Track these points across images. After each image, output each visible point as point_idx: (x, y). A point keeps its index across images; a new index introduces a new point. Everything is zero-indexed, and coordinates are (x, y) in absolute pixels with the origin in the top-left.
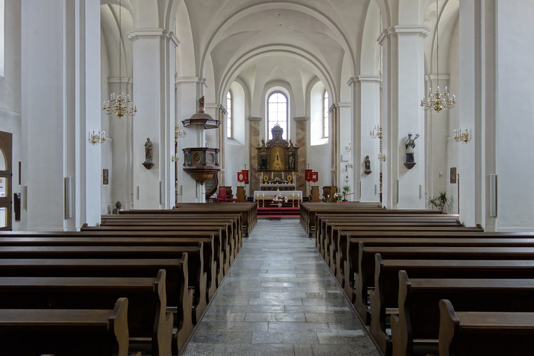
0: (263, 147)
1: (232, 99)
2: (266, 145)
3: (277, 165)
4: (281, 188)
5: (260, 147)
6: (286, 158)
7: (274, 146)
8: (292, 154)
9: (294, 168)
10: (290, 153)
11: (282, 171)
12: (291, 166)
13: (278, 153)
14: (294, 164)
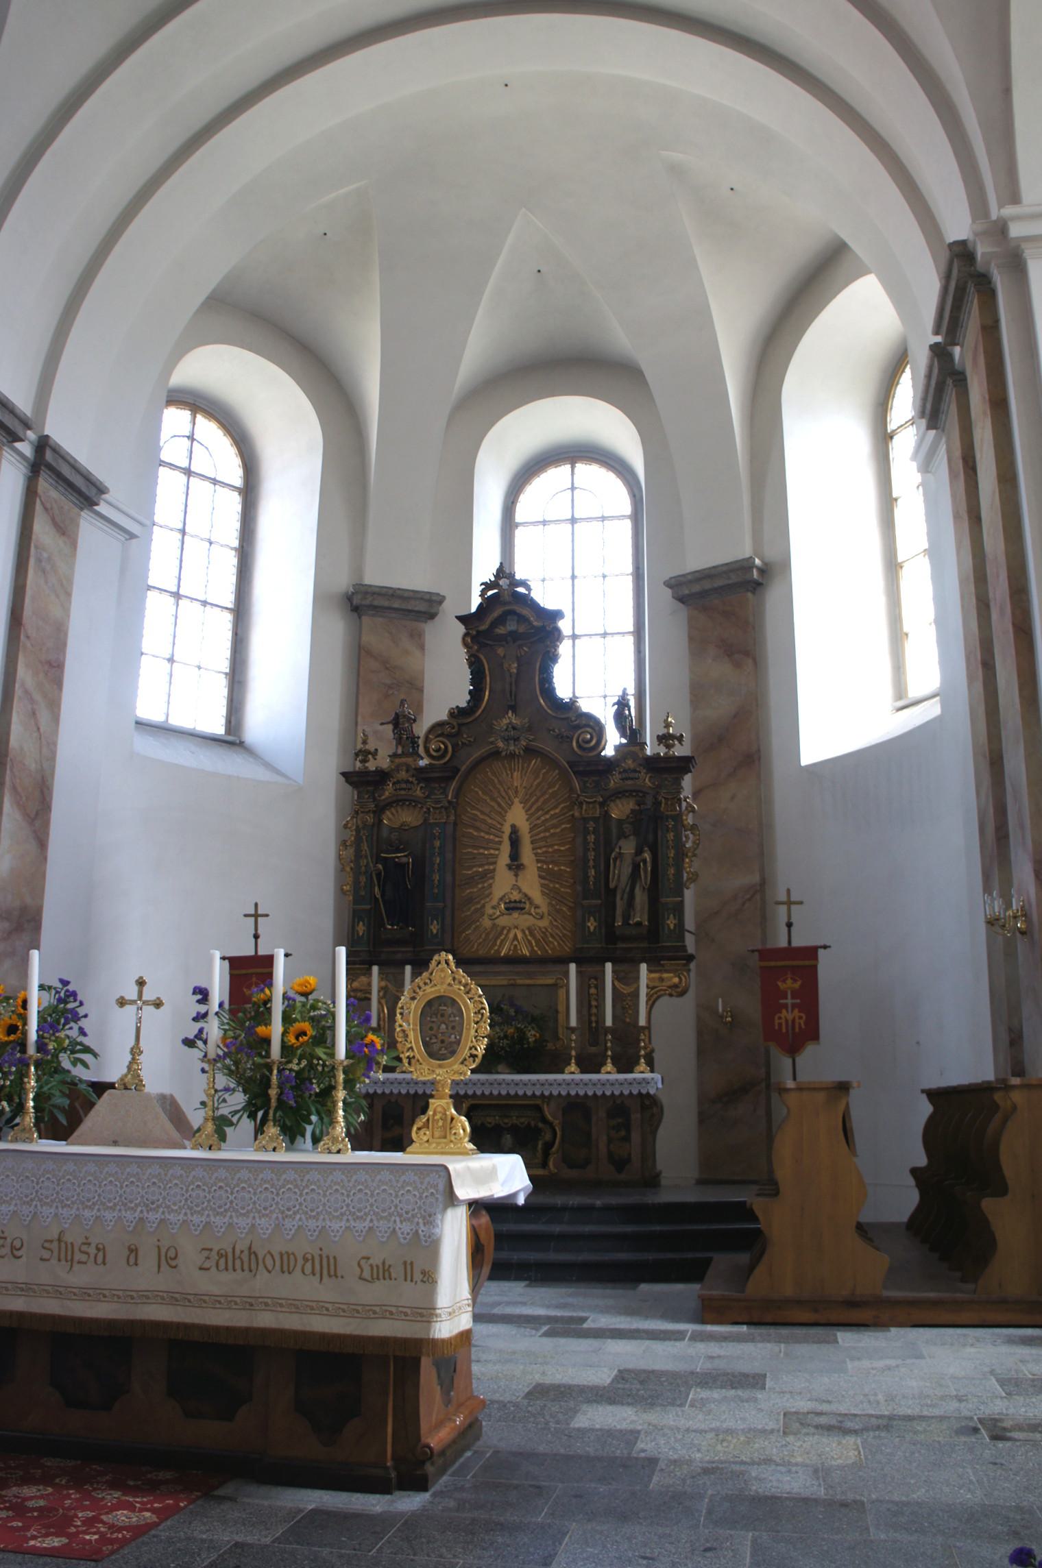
0: (398, 769)
1: (250, 492)
2: (421, 750)
3: (514, 907)
4: (538, 1108)
5: (371, 766)
6: (586, 850)
7: (482, 760)
8: (636, 818)
9: (654, 931)
10: (620, 810)
11: (565, 961)
12: (626, 918)
13: (517, 816)
14: (654, 892)
